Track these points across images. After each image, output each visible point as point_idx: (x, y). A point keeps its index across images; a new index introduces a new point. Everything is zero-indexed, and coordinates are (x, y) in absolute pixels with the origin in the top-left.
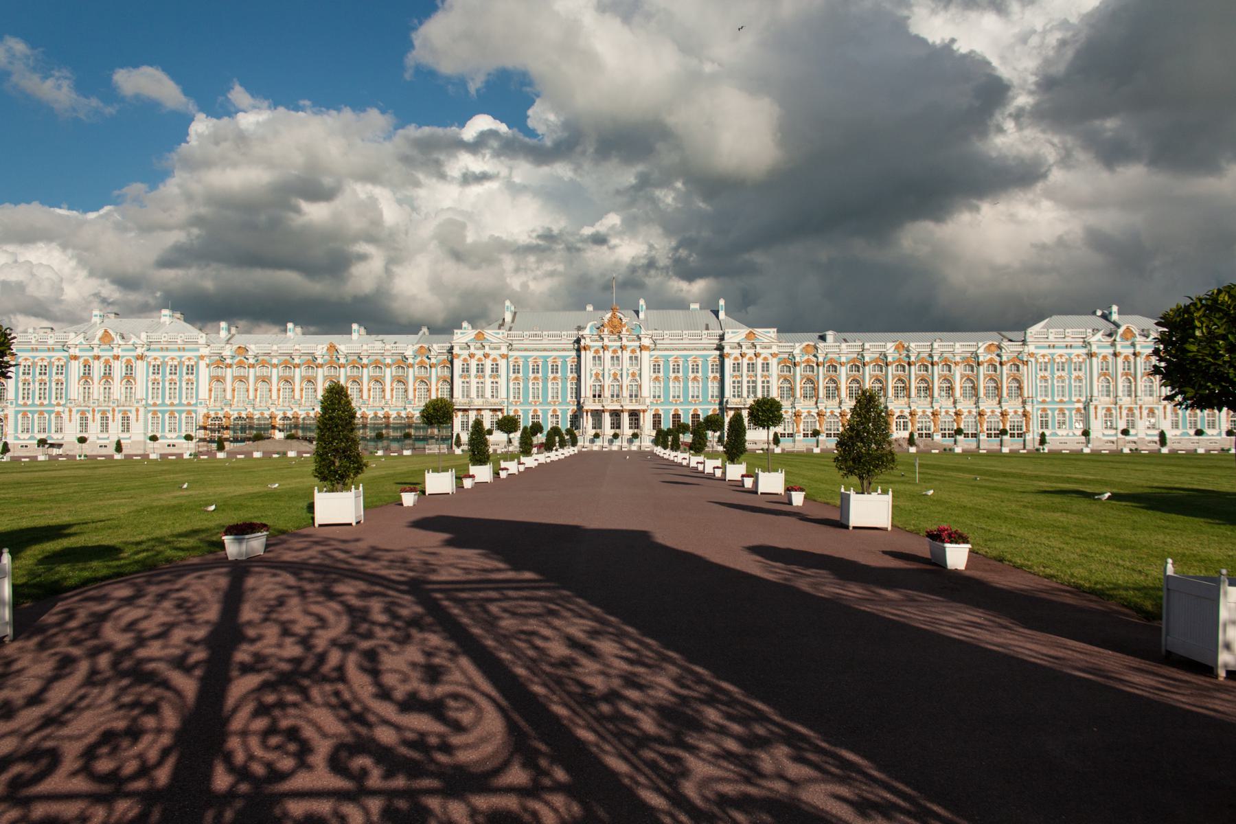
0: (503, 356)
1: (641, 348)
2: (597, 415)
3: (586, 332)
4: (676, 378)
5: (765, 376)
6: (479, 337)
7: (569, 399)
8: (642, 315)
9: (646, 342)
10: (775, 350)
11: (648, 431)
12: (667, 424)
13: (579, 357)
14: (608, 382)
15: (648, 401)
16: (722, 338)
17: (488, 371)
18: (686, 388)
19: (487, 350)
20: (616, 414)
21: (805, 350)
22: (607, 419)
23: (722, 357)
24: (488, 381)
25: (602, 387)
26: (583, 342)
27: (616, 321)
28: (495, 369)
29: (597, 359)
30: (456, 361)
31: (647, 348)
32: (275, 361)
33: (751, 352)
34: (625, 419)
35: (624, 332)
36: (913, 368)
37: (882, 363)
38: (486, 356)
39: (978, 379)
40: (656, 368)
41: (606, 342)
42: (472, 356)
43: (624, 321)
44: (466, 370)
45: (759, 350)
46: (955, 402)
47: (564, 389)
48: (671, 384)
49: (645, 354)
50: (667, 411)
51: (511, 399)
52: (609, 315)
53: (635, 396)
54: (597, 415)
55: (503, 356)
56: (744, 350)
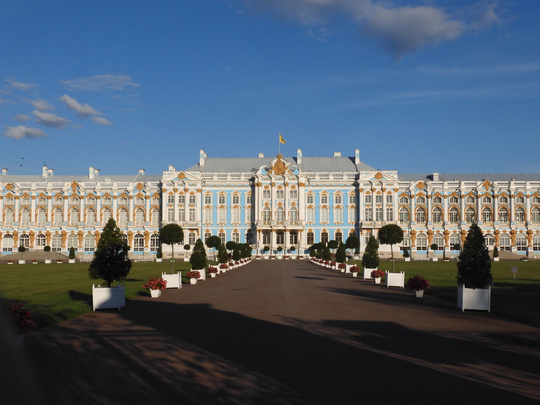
0: (199, 191)
1: (299, 185)
2: (267, 233)
3: (259, 173)
4: (325, 207)
5: (389, 206)
6: (181, 176)
8: (299, 161)
9: (302, 180)
10: (396, 186)
11: (304, 244)
12: (318, 240)
13: (253, 191)
14: (275, 209)
15: (304, 223)
16: (357, 177)
19: (187, 186)
20: (280, 233)
21: (419, 186)
23: (358, 191)
24: (187, 209)
25: (270, 213)
26: (256, 179)
27: (281, 166)
29: (267, 193)
31: (303, 185)
32: (34, 194)
33: (378, 188)
34: (288, 235)
35: (286, 173)
36: (463, 199)
37: (474, 196)
38: (186, 190)
39: (411, 209)
40: (310, 199)
41: (273, 180)
42: (175, 190)
43: (287, 164)
44: (171, 200)
45: (384, 186)
46: (526, 225)
49: (302, 189)
50: (318, 231)
51: (204, 222)
52: (275, 161)
53: (296, 219)
54: (267, 233)
55: (199, 191)
56: (374, 186)
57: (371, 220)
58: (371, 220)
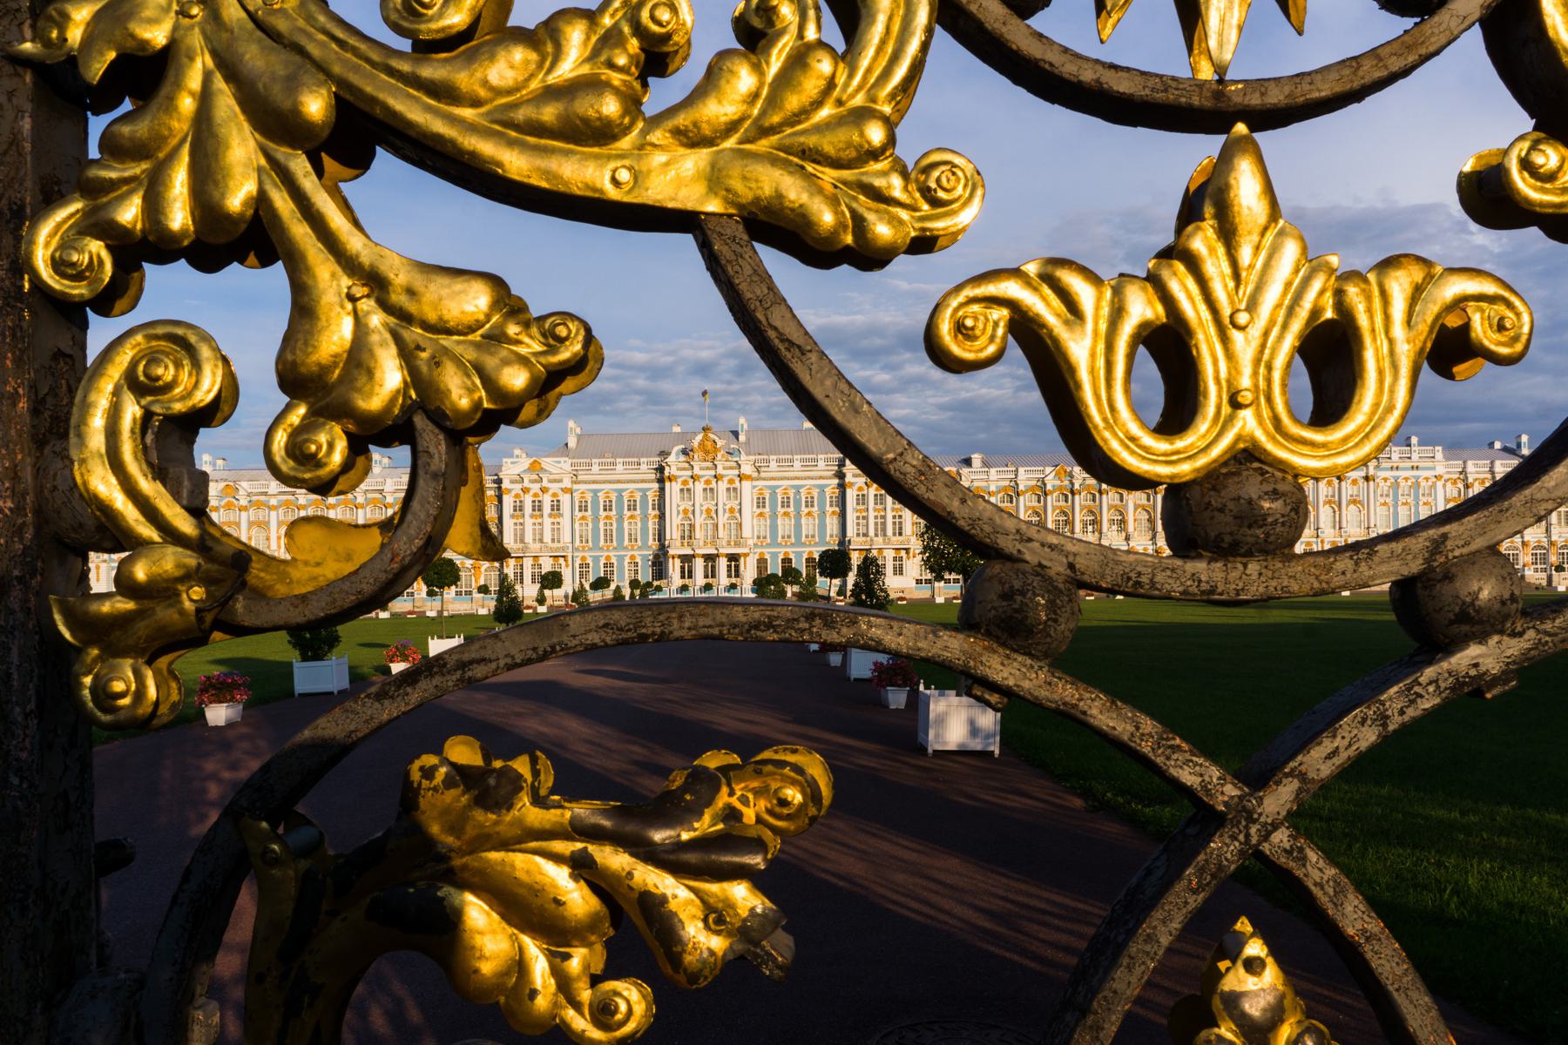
3: (671, 459)
4: (786, 514)
7: (651, 542)
8: (742, 438)
9: (747, 469)
13: (662, 489)
14: (699, 520)
15: (750, 542)
17: (547, 509)
18: (798, 526)
19: (545, 483)
20: (710, 558)
22: (699, 565)
23: (842, 487)
24: (547, 521)
25: (692, 526)
27: (709, 444)
28: (556, 507)
29: (686, 492)
30: (505, 498)
31: (749, 478)
32: (273, 502)
34: (723, 563)
37: (1042, 491)
40: (761, 503)
42: (525, 490)
43: (720, 443)
44: (519, 508)
46: (1127, 539)
47: (645, 529)
48: (803, 521)
49: (747, 485)
50: (774, 555)
51: (577, 543)
52: (699, 437)
54: (687, 559)
57: (865, 535)
58: (865, 535)
